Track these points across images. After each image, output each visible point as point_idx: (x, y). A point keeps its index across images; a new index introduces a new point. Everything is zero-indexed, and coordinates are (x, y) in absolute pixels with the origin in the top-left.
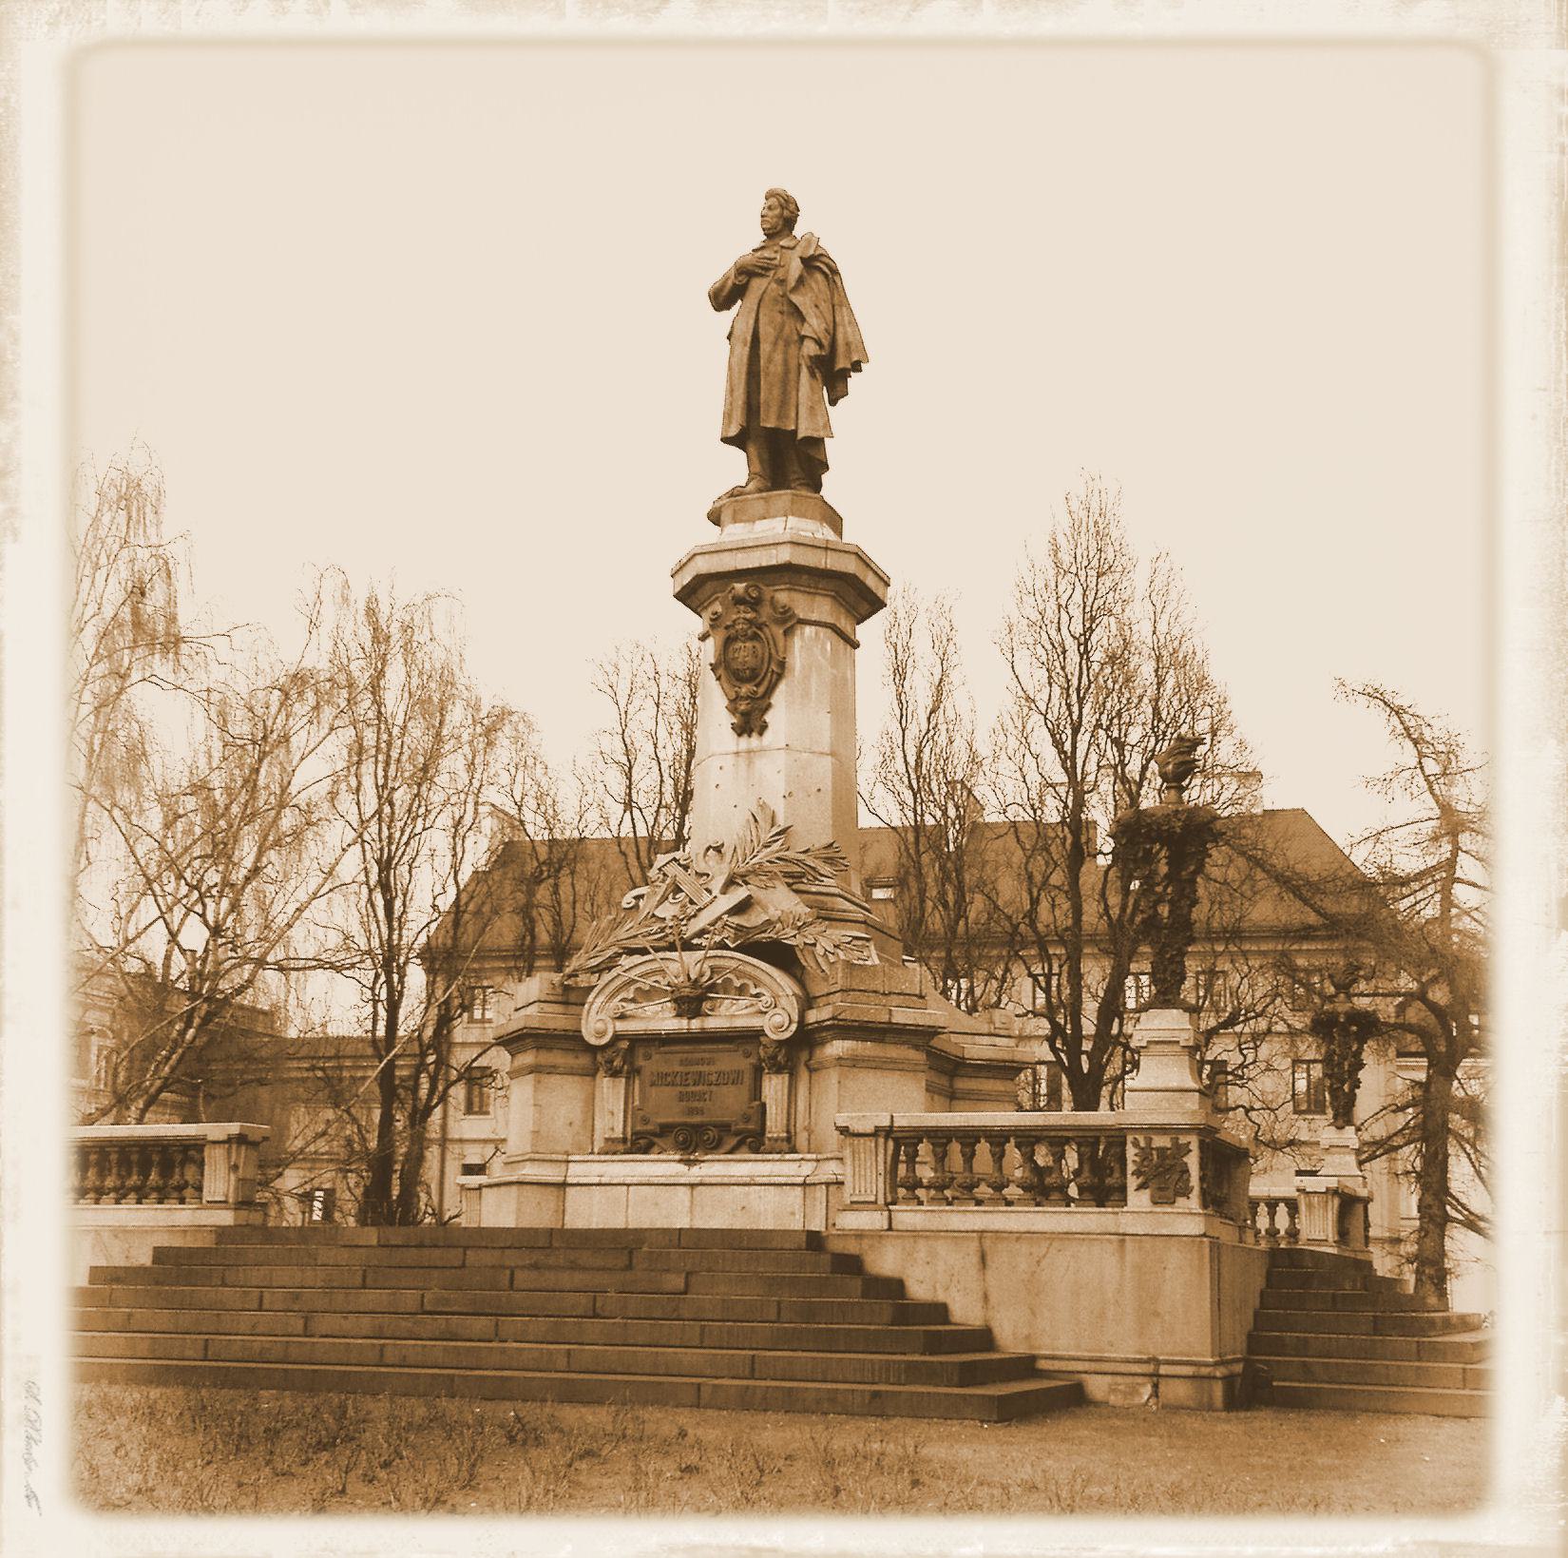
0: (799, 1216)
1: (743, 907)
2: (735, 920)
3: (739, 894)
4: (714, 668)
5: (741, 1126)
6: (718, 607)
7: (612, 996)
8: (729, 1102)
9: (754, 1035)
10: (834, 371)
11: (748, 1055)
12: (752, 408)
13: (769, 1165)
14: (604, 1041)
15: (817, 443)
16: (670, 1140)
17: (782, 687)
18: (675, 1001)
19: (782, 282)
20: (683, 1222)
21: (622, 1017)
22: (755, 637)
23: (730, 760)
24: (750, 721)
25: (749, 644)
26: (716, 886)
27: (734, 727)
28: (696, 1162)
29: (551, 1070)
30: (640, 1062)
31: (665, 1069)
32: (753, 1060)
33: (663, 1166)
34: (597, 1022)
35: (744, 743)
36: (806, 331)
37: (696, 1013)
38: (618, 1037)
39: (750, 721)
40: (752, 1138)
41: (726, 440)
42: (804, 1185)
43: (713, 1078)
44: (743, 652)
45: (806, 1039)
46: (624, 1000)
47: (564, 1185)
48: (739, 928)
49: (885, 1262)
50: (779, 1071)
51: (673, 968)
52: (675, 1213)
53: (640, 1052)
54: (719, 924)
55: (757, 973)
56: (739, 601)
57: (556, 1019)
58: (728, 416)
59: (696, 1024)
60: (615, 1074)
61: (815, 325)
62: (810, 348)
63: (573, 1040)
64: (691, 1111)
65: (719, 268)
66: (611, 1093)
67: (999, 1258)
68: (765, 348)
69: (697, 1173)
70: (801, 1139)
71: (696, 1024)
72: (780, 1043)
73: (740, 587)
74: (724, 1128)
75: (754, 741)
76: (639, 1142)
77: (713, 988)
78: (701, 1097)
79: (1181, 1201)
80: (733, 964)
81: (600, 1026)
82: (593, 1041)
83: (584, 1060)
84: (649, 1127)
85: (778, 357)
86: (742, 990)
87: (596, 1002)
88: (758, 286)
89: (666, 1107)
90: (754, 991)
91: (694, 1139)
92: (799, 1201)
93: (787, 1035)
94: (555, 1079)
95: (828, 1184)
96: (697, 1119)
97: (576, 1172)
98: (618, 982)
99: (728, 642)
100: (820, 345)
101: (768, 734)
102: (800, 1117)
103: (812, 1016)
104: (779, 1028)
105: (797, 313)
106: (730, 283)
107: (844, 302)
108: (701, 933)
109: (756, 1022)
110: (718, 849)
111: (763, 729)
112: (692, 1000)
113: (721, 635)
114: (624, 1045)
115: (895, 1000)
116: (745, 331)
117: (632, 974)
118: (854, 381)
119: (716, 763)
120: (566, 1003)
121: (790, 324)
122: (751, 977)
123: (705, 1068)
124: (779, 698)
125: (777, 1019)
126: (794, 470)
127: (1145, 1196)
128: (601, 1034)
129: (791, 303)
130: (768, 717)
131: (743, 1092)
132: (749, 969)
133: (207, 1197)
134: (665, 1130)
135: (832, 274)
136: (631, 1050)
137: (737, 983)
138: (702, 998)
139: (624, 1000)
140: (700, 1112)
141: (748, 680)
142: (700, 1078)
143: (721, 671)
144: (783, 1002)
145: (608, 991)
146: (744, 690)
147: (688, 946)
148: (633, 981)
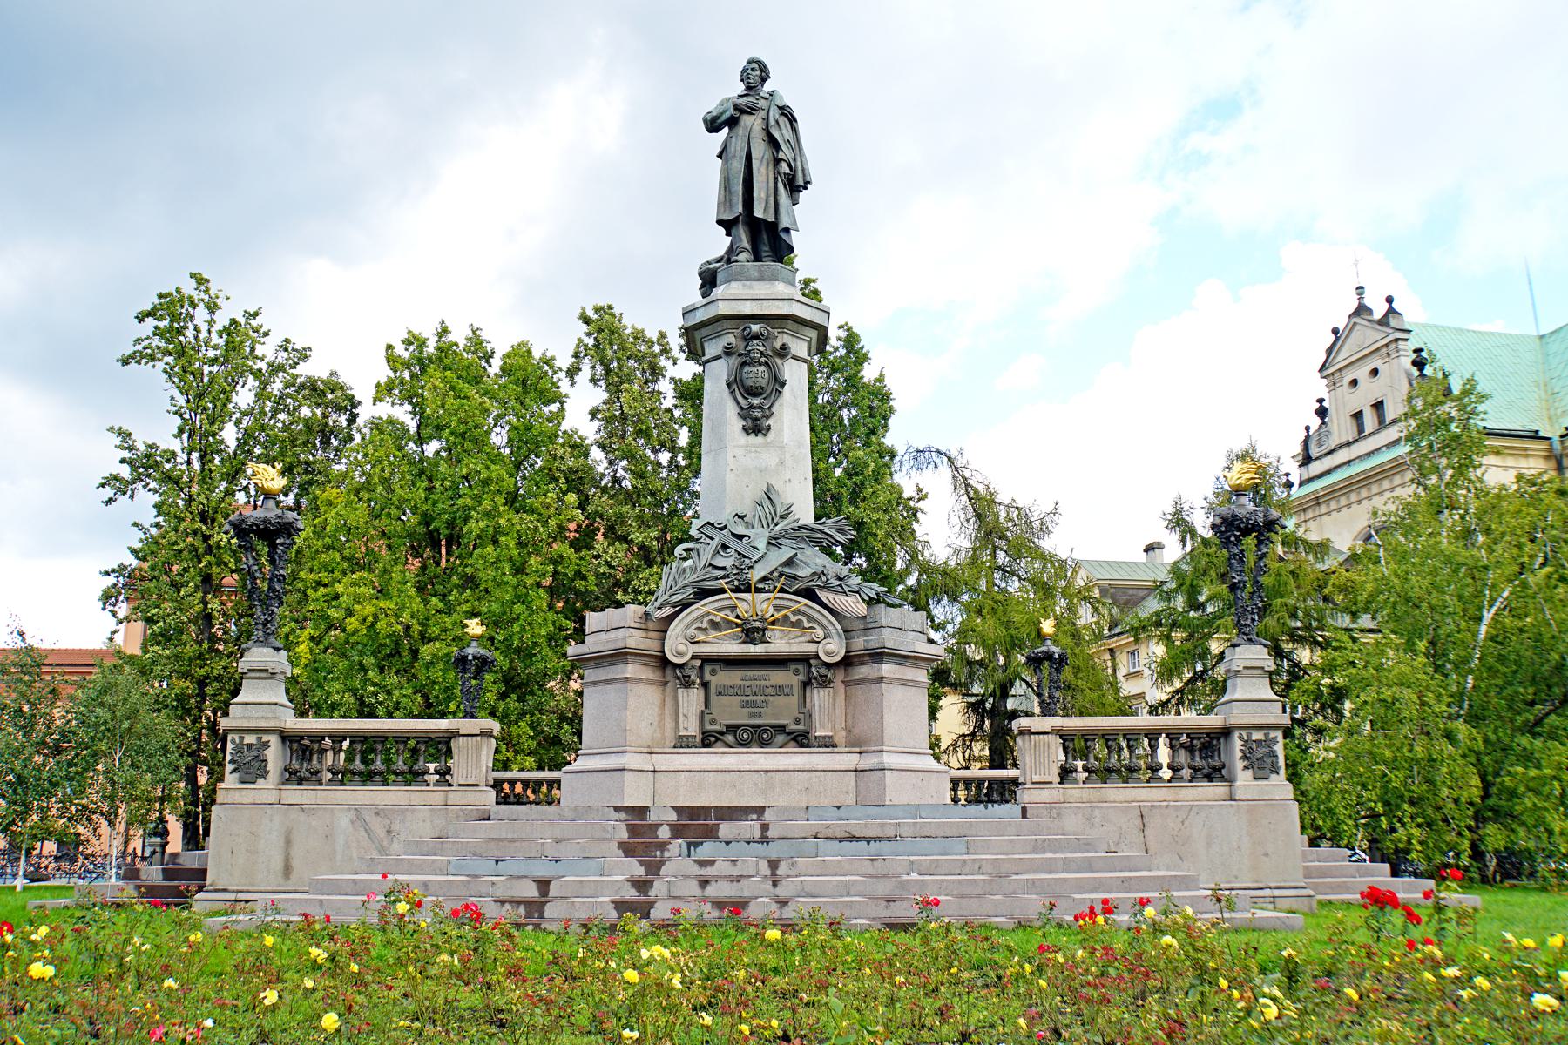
1: (790, 562)
2: (786, 570)
3: (787, 553)
4: (729, 385)
5: (793, 727)
6: (731, 339)
7: (687, 628)
8: (782, 711)
9: (805, 660)
10: (795, 185)
11: (796, 673)
15: (787, 230)
16: (730, 738)
19: (766, 120)
24: (756, 426)
25: (762, 368)
26: (762, 545)
27: (745, 430)
29: (638, 680)
30: (708, 677)
31: (728, 682)
32: (802, 677)
36: (781, 155)
38: (694, 657)
39: (756, 426)
40: (802, 739)
41: (720, 222)
43: (769, 691)
45: (848, 662)
46: (699, 629)
48: (795, 578)
50: (825, 683)
53: (708, 669)
55: (811, 612)
56: (756, 337)
60: (687, 683)
61: (785, 153)
63: (663, 662)
64: (751, 716)
65: (711, 105)
66: (691, 700)
67: (1154, 823)
72: (828, 666)
73: (755, 328)
74: (781, 729)
75: (760, 439)
76: (708, 740)
77: (773, 623)
79: (1273, 776)
80: (796, 606)
81: (682, 648)
84: (717, 727)
86: (793, 625)
87: (676, 628)
88: (746, 120)
90: (806, 625)
92: (853, 783)
97: (662, 762)
100: (789, 165)
103: (859, 643)
104: (828, 654)
106: (727, 115)
108: (764, 579)
109: (810, 648)
110: (742, 517)
113: (734, 361)
114: (698, 663)
116: (738, 147)
117: (707, 609)
118: (803, 196)
122: (804, 614)
123: (763, 683)
125: (830, 647)
126: (765, 249)
127: (1249, 773)
128: (680, 655)
130: (770, 422)
131: (794, 700)
132: (805, 609)
134: (732, 729)
135: (793, 121)
136: (701, 667)
137: (793, 619)
138: (765, 630)
139: (699, 629)
140: (760, 716)
141: (755, 395)
142: (761, 691)
146: (756, 402)
147: (748, 590)
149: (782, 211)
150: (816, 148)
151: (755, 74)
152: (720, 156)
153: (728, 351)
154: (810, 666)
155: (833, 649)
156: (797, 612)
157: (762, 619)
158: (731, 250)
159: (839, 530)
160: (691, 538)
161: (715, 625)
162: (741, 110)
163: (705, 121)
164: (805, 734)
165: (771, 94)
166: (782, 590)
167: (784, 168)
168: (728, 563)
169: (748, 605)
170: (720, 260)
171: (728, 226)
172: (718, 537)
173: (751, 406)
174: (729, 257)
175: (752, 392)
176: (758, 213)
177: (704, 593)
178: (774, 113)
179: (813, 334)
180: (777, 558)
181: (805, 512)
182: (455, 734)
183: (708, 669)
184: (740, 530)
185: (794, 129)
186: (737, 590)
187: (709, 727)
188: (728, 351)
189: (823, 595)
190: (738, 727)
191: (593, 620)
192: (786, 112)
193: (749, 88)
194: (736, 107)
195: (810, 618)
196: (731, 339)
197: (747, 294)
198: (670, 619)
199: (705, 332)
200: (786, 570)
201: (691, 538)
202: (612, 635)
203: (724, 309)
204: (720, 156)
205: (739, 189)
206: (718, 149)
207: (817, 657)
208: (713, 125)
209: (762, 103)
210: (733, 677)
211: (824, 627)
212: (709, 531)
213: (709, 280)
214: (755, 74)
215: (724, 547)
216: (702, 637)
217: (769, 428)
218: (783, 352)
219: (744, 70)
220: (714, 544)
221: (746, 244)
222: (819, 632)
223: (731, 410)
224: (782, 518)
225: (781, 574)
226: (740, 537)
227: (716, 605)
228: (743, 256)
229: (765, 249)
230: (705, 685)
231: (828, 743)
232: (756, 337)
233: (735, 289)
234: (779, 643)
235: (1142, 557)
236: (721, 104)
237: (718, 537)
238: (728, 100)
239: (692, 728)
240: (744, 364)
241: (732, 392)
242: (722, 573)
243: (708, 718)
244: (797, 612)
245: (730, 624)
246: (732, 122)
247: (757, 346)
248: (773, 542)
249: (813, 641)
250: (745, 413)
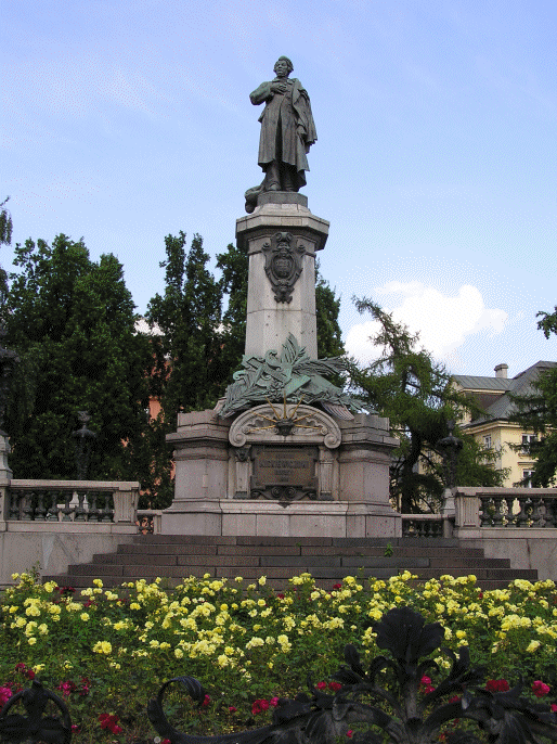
0: (344, 530)
1: (306, 385)
2: (305, 390)
3: (305, 379)
4: (266, 271)
8: (300, 476)
10: (308, 140)
12: (279, 152)
13: (329, 507)
14: (241, 445)
15: (303, 171)
16: (267, 494)
17: (298, 282)
18: (277, 427)
19: (290, 99)
20: (285, 534)
21: (249, 433)
22: (290, 258)
23: (273, 313)
24: (283, 296)
26: (288, 372)
27: (276, 299)
28: (289, 504)
33: (273, 506)
34: (238, 434)
35: (280, 306)
37: (286, 434)
38: (247, 443)
39: (283, 296)
40: (312, 494)
41: (259, 164)
42: (346, 515)
44: (283, 264)
47: (222, 513)
48: (311, 395)
49: (489, 552)
51: (277, 411)
52: (282, 529)
54: (298, 392)
56: (284, 240)
57: (218, 435)
58: (261, 154)
59: (288, 439)
60: (243, 460)
62: (301, 130)
68: (284, 127)
69: (290, 509)
70: (335, 494)
71: (288, 439)
73: (284, 234)
74: (299, 488)
75: (285, 306)
76: (256, 493)
78: (286, 473)
80: (312, 413)
82: (235, 445)
83: (224, 453)
85: (289, 131)
86: (309, 424)
89: (269, 478)
90: (317, 425)
91: (284, 493)
93: (336, 446)
94: (213, 462)
95: (365, 515)
96: (282, 484)
97: (225, 507)
98: (248, 417)
99: (276, 257)
101: (292, 304)
102: (334, 484)
103: (349, 438)
104: (331, 443)
105: (295, 113)
106: (267, 94)
107: (310, 113)
108: (291, 396)
109: (320, 439)
110: (274, 355)
111: (289, 300)
112: (284, 428)
113: (270, 255)
115: (380, 432)
116: (273, 115)
117: (257, 413)
119: (266, 313)
120: (217, 425)
121: (293, 118)
124: (298, 287)
128: (239, 441)
129: (293, 109)
130: (292, 295)
133: (115, 519)
134: (269, 488)
135: (307, 99)
136: (251, 449)
138: (292, 426)
143: (270, 271)
144: (334, 430)
145: (242, 421)
146: (283, 281)
147: (281, 401)
148: (256, 416)
149: (300, 157)
150: (322, 116)
151: (284, 68)
152: (260, 120)
153: (266, 249)
154: (318, 451)
155: (333, 439)
156: (312, 417)
157: (290, 420)
158: (266, 182)
159: (335, 365)
160: (243, 368)
161: (260, 423)
162: (274, 91)
163: (252, 98)
164: (315, 492)
165: (294, 80)
166: (303, 403)
167: (301, 130)
168: (267, 384)
169: (284, 411)
170: (258, 188)
171: (265, 167)
172: (260, 367)
173: (281, 284)
174: (265, 186)
175: (279, 275)
176: (285, 160)
177: (254, 404)
178: (296, 95)
179: (318, 238)
180: (297, 383)
181: (314, 357)
182: (116, 490)
183: (255, 450)
184: (273, 362)
185: (308, 105)
186: (274, 402)
187: (255, 487)
188: (266, 249)
189: (325, 406)
190: (272, 487)
191: (182, 418)
192: (304, 95)
193: (279, 77)
194: (273, 90)
195: (319, 420)
196: (268, 240)
197: (275, 212)
198: (233, 418)
199: (249, 236)
200: (305, 390)
201: (243, 368)
202: (197, 427)
203: (264, 221)
204: (260, 120)
205: (273, 144)
206: (259, 117)
207: (323, 444)
208: (256, 100)
209: (288, 88)
210: (273, 456)
211: (328, 427)
212: (253, 363)
213: (252, 202)
214: (284, 68)
215: (265, 374)
216: (252, 429)
217: (291, 299)
218: (301, 251)
219: (277, 65)
220: (258, 372)
221: (276, 178)
222: (324, 428)
223: (268, 287)
224: (300, 355)
225: (302, 393)
226: (275, 368)
227: (261, 411)
228: (274, 187)
229: (288, 183)
230: (252, 460)
231: (328, 498)
232: (284, 240)
233: (269, 208)
234: (300, 435)
235: (493, 374)
236: (262, 86)
237: (260, 367)
238: (266, 84)
239: (245, 486)
240: (276, 257)
241: (268, 275)
242: (264, 391)
243: (255, 481)
244: (312, 417)
245: (270, 423)
246: (269, 100)
247: (284, 246)
248: (296, 371)
249: (321, 435)
250: (275, 289)
